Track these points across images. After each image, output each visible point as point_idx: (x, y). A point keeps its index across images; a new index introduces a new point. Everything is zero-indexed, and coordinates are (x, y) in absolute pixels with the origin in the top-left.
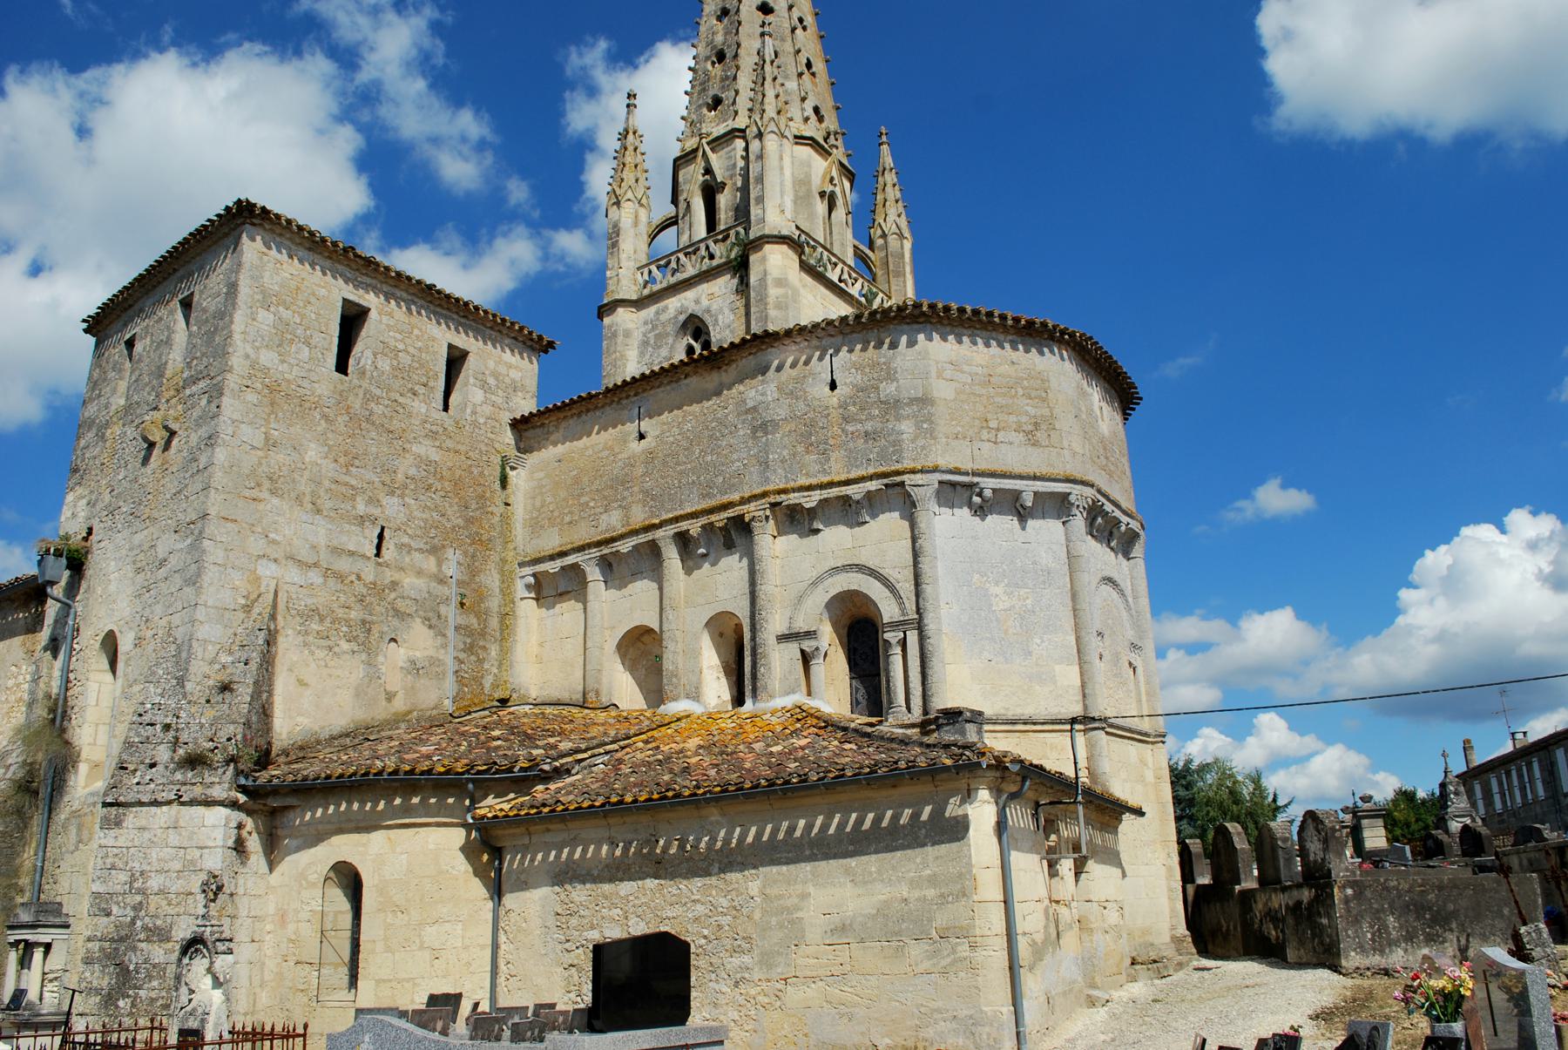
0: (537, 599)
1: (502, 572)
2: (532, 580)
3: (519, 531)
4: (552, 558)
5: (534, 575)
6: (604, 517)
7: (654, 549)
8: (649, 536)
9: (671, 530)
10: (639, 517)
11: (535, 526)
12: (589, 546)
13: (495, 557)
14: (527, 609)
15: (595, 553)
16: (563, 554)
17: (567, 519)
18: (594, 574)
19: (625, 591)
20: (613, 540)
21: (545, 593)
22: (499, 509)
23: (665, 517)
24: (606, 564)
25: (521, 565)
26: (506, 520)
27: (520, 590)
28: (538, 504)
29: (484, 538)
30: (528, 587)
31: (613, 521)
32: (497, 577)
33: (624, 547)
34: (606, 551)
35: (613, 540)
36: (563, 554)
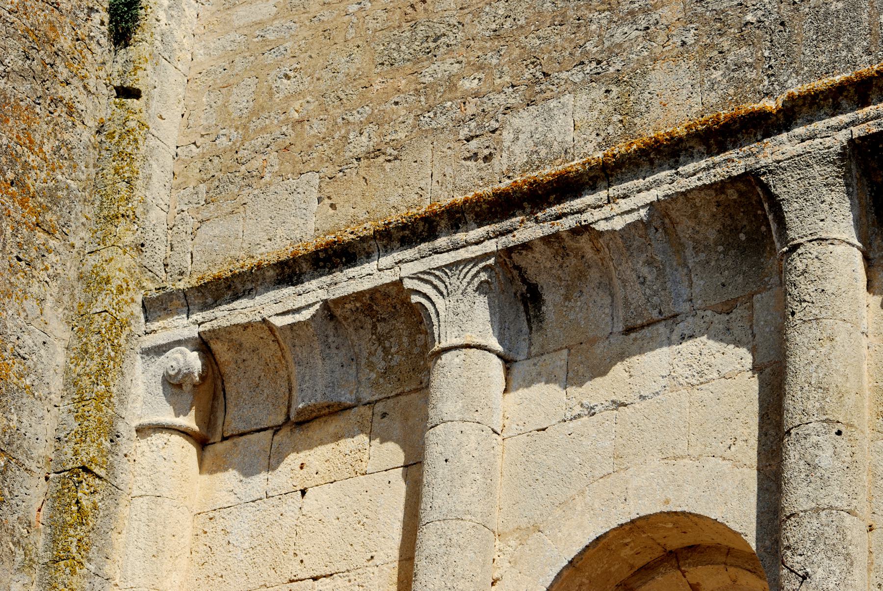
0: (202, 442)
1: (80, 319)
2: (194, 361)
3: (159, 193)
4: (288, 272)
5: (203, 345)
6: (524, 120)
7: (751, 223)
8: (734, 162)
9: (834, 132)
10: (677, 101)
11: (224, 178)
12: (456, 217)
13: (63, 262)
14: (162, 476)
15: (480, 241)
16: (336, 256)
17: (362, 143)
18: (465, 320)
19: (597, 390)
20: (567, 186)
21: (234, 419)
22: (99, 107)
23: (796, 87)
24: (518, 292)
25: (156, 307)
26: (119, 146)
27: (142, 396)
28: (241, 99)
29: (36, 181)
30: (173, 385)
31: (568, 128)
32: (61, 333)
33: (614, 211)
34: (528, 231)
35: (567, 186)
36: (336, 256)
